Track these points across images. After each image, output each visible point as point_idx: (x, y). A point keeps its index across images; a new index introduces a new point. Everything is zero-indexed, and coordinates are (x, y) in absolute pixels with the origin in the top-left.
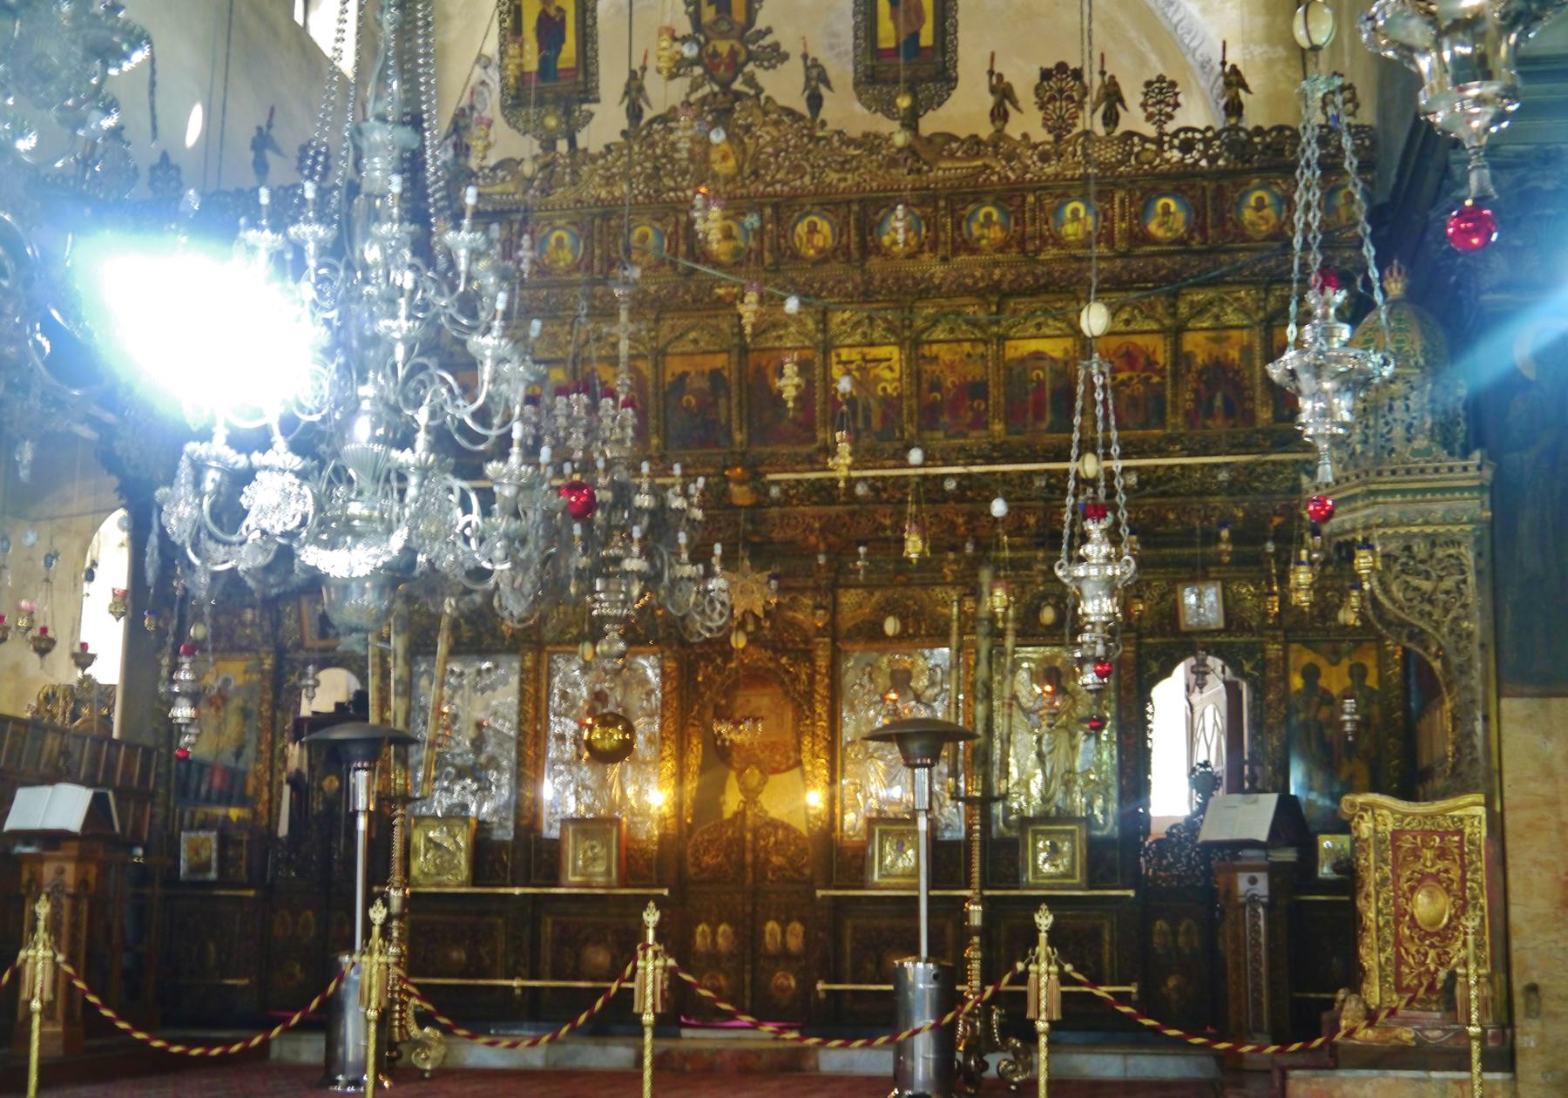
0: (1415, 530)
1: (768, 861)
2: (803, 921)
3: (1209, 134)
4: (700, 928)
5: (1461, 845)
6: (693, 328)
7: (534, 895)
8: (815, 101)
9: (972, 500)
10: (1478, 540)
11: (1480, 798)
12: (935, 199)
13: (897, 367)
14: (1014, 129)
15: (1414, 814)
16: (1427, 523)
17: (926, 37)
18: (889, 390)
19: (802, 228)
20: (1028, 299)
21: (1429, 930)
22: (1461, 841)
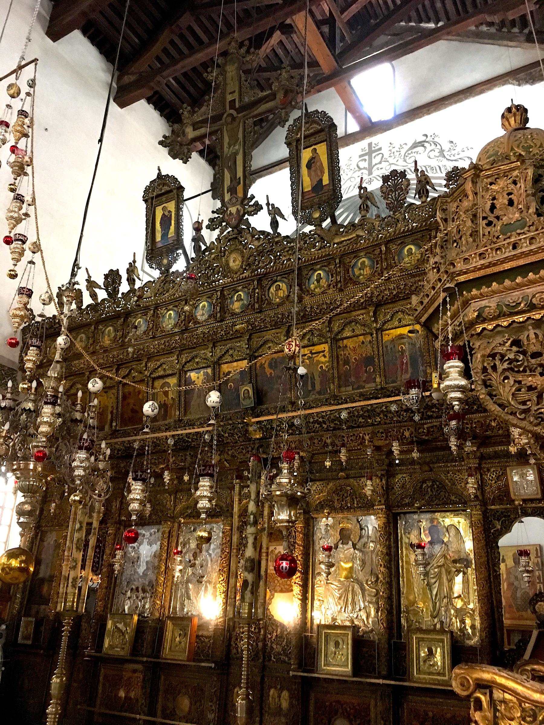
0: (520, 318)
2: (288, 690)
7: (154, 662)
9: (373, 425)
12: (334, 259)
13: (327, 355)
17: (326, 180)
19: (273, 289)
20: (391, 306)
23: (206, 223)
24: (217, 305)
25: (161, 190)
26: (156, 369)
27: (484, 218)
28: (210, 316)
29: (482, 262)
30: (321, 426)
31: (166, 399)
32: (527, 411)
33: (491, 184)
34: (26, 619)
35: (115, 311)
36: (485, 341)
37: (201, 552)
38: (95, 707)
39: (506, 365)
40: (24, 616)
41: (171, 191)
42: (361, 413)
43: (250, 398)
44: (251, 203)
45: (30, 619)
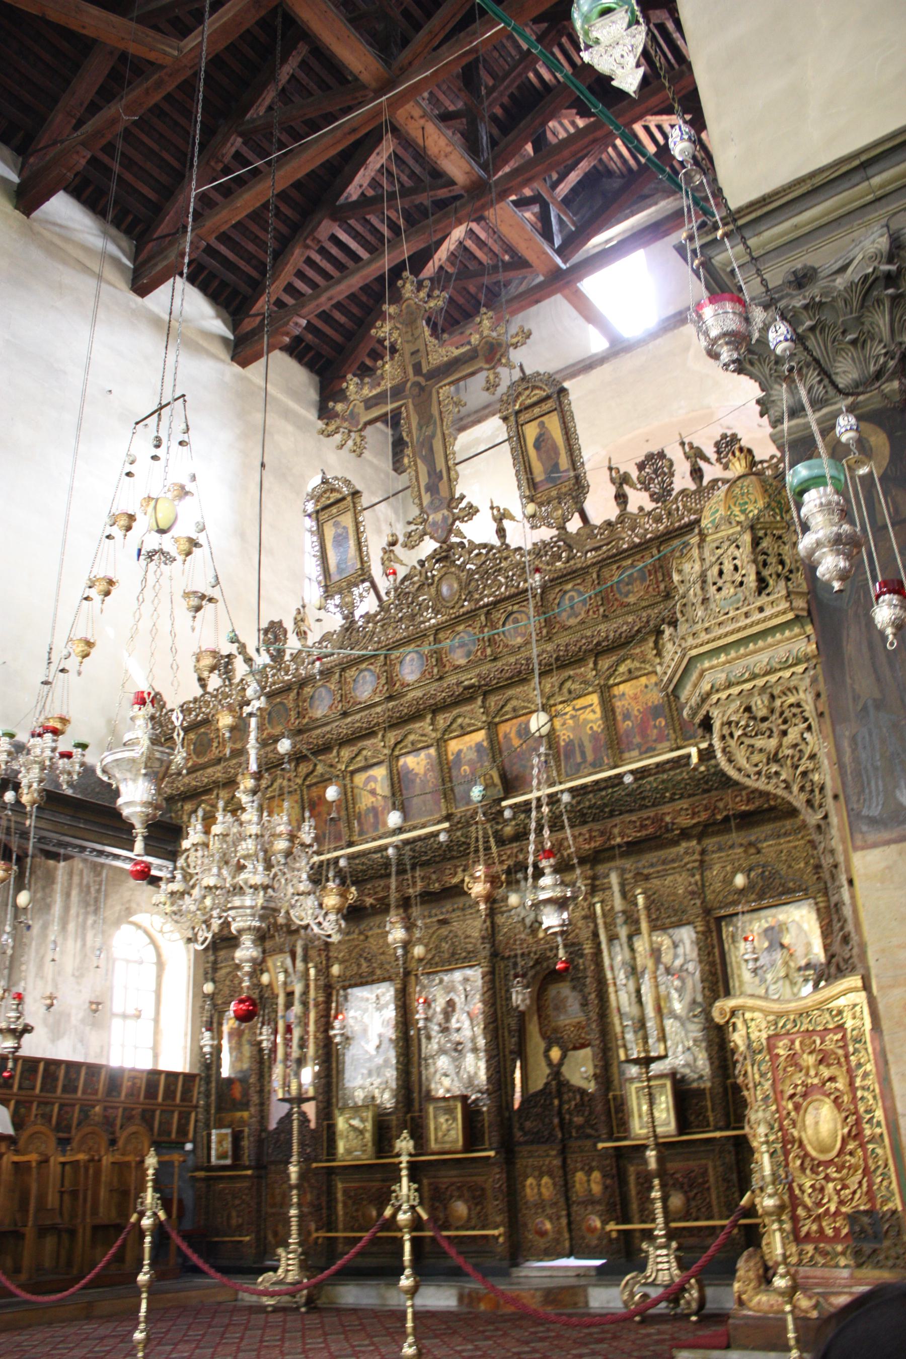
1: (571, 1121)
3: (775, 460)
4: (530, 1181)
5: (845, 1047)
6: (459, 716)
8: (501, 532)
10: (814, 680)
11: (855, 981)
13: (598, 709)
14: (632, 508)
15: (787, 1013)
16: (754, 677)
17: (564, 462)
18: (595, 728)
21: (823, 1157)
22: (844, 1037)
23: (401, 539)
24: (432, 657)
25: (329, 498)
26: (354, 758)
27: (715, 584)
28: (423, 673)
29: (708, 636)
30: (602, 811)
31: (374, 799)
32: (759, 773)
33: (717, 548)
34: (218, 1131)
35: (283, 682)
36: (722, 709)
37: (454, 1010)
38: (337, 1231)
39: (740, 732)
40: (216, 1128)
41: (343, 499)
42: (655, 785)
43: (495, 785)
44: (462, 505)
45: (224, 1131)
